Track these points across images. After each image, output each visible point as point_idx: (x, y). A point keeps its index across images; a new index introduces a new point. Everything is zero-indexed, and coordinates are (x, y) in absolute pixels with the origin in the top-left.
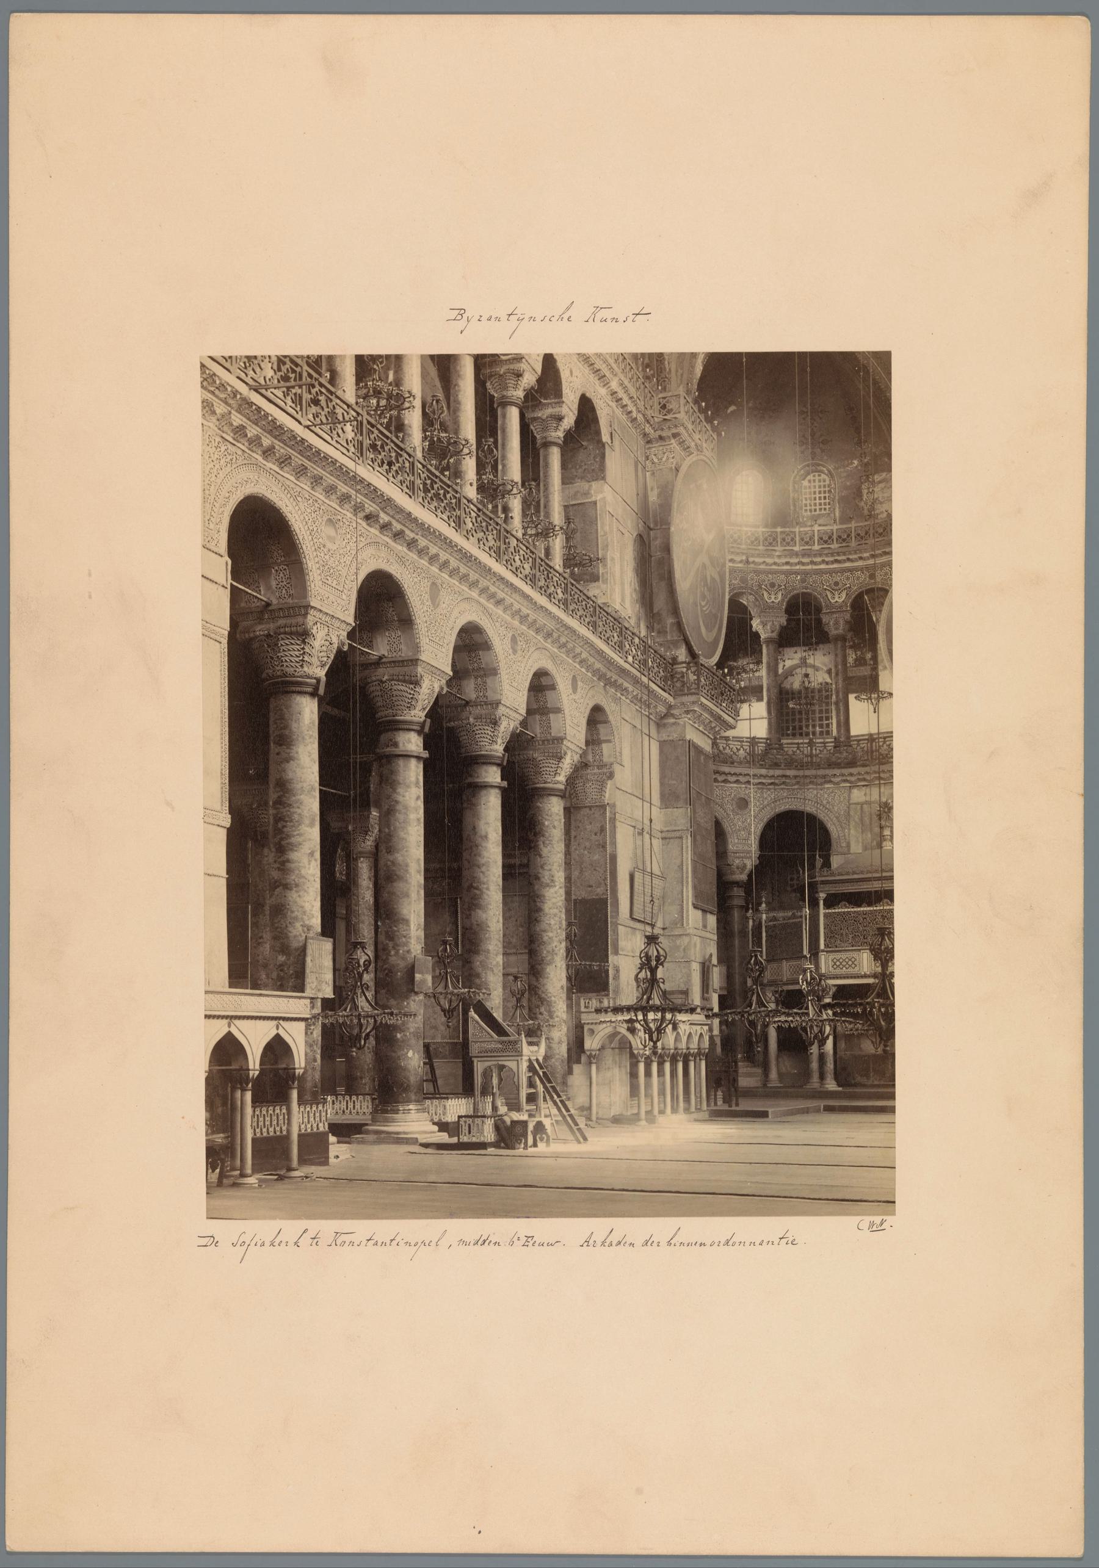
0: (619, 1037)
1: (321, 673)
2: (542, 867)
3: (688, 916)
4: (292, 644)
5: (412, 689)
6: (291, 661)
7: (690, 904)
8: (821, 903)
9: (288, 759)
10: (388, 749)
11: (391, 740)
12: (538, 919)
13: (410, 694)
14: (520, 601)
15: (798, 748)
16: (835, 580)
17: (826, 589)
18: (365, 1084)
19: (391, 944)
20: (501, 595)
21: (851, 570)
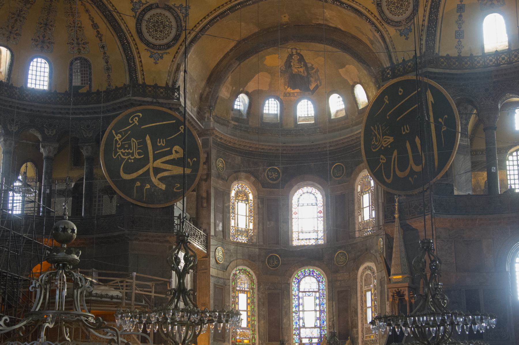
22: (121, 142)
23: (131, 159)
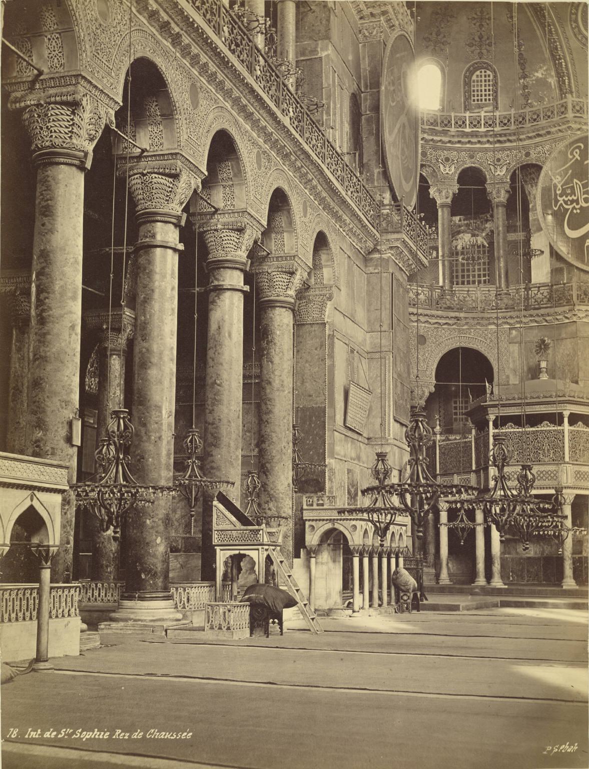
0: (335, 533)
1: (90, 147)
2: (273, 372)
3: (389, 427)
4: (62, 114)
6: (60, 132)
7: (392, 417)
8: (491, 424)
9: (51, 231)
10: (147, 240)
11: (150, 232)
12: (269, 421)
13: (169, 187)
14: (267, 119)
15: (468, 294)
16: (497, 157)
18: (110, 573)
19: (143, 430)
20: (251, 109)
21: (509, 149)
22: (562, 186)
23: (576, 209)
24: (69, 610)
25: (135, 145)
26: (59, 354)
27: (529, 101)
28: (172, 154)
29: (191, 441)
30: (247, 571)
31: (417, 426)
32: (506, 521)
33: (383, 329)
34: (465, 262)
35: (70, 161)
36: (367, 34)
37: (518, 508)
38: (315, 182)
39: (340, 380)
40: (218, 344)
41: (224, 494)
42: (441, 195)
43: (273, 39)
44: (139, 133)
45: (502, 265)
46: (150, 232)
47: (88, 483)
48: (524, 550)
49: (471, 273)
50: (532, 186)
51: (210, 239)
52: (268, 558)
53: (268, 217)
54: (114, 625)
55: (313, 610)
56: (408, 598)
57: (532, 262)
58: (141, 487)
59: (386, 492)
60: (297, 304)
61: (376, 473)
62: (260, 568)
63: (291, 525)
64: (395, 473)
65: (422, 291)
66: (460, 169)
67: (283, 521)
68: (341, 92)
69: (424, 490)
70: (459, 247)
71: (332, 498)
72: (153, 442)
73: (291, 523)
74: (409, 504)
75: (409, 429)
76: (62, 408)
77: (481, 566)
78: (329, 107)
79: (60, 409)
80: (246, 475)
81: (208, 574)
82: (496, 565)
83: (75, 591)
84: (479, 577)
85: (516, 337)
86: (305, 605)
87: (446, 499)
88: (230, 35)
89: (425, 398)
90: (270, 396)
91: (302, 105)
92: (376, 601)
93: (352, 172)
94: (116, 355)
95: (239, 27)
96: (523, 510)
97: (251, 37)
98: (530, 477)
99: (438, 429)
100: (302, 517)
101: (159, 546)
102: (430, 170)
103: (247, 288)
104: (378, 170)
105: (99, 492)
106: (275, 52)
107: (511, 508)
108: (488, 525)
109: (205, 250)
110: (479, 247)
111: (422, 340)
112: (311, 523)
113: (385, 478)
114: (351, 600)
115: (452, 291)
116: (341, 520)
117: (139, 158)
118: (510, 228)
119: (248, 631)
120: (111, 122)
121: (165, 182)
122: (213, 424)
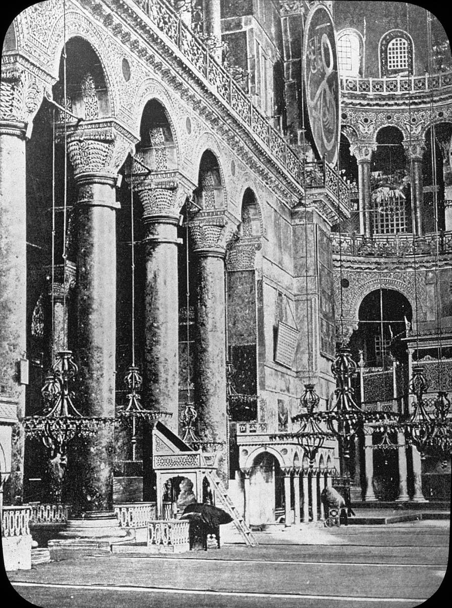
1: (30, 119)
5: (107, 148)
8: (410, 356)
11: (88, 192)
13: (105, 152)
15: (388, 242)
17: (406, 124)
20: (179, 79)
24: (21, 529)
25: (71, 116)
26: (6, 303)
27: (442, 66)
28: (106, 122)
29: (131, 378)
30: (185, 491)
31: (343, 361)
32: (425, 442)
33: (309, 274)
34: (384, 213)
35: (11, 131)
36: (288, 9)
37: (436, 430)
38: (242, 144)
39: (269, 322)
40: (153, 291)
41: (163, 423)
42: (361, 154)
43: (200, 15)
44: (75, 104)
45: (418, 215)
46: (88, 192)
47: (36, 417)
48: (443, 468)
49: (390, 223)
50: (445, 143)
51: (146, 198)
52: (205, 480)
53: (199, 177)
54: (62, 541)
55: (248, 526)
56: (336, 514)
57: (446, 212)
58: (85, 419)
59: (315, 419)
60: (228, 254)
61: (305, 403)
62: (198, 490)
63: (226, 450)
64: (322, 403)
65: (345, 240)
66: (378, 129)
67: (218, 447)
68: (265, 62)
69: (350, 417)
70: (379, 200)
71: (264, 426)
72: (96, 379)
73: (226, 447)
74: (336, 430)
75: (334, 363)
76: (11, 351)
77: (404, 484)
78: (253, 77)
79: (9, 352)
80: (182, 408)
81: (150, 496)
82: (418, 482)
83: (26, 513)
84: (402, 494)
85: (432, 279)
86: (241, 521)
87: (371, 424)
88: (158, 14)
89: (349, 335)
90: (204, 336)
91: (228, 74)
92: (307, 517)
93: (276, 133)
94: (59, 302)
95: (167, 7)
96: (441, 432)
97: (178, 15)
98: (446, 402)
99: (361, 362)
100: (236, 443)
101: (104, 472)
102: (349, 130)
103: (181, 241)
104: (301, 131)
105: (46, 424)
106: (201, 27)
107: (430, 431)
108: (409, 446)
109: (140, 208)
110: (397, 199)
111: (345, 283)
112: (244, 448)
113: (313, 407)
114: (283, 517)
115: (372, 239)
116: (272, 444)
117: (76, 126)
118: (427, 181)
119: (188, 545)
120: (49, 96)
121: (101, 147)
122: (151, 362)
